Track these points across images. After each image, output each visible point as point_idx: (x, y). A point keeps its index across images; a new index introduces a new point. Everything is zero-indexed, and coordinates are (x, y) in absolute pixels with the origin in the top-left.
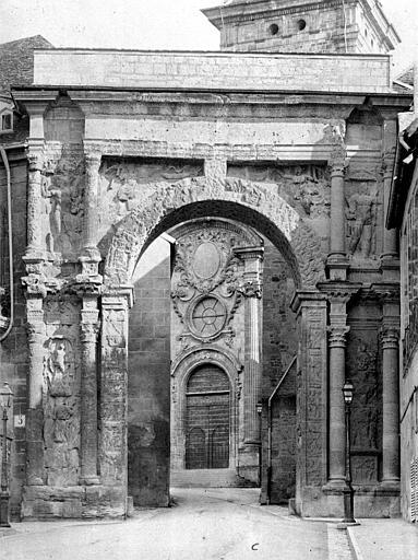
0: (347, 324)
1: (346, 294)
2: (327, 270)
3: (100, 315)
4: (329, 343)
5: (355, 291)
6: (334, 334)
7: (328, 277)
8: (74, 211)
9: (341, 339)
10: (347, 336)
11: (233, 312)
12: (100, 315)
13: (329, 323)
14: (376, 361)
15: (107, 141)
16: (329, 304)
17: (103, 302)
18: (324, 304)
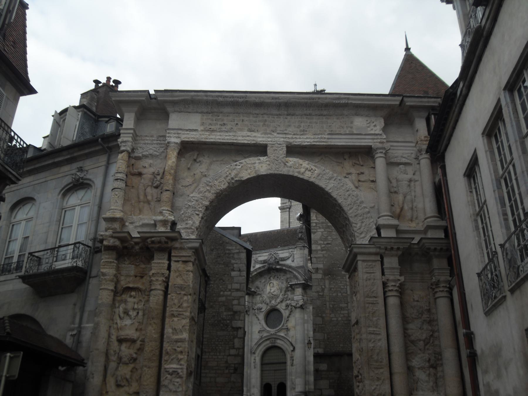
0: (401, 275)
1: (398, 249)
2: (378, 229)
3: (169, 268)
4: (385, 293)
5: (406, 246)
6: (390, 284)
7: (379, 233)
8: (155, 185)
9: (396, 288)
10: (401, 286)
11: (288, 317)
12: (169, 268)
13: (383, 274)
14: (429, 311)
15: (187, 130)
16: (382, 258)
17: (173, 254)
18: (379, 258)
